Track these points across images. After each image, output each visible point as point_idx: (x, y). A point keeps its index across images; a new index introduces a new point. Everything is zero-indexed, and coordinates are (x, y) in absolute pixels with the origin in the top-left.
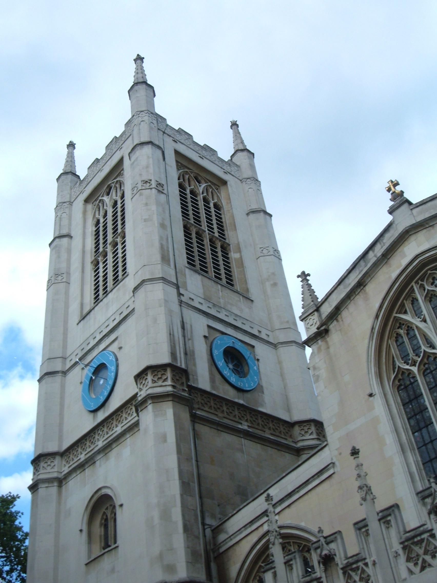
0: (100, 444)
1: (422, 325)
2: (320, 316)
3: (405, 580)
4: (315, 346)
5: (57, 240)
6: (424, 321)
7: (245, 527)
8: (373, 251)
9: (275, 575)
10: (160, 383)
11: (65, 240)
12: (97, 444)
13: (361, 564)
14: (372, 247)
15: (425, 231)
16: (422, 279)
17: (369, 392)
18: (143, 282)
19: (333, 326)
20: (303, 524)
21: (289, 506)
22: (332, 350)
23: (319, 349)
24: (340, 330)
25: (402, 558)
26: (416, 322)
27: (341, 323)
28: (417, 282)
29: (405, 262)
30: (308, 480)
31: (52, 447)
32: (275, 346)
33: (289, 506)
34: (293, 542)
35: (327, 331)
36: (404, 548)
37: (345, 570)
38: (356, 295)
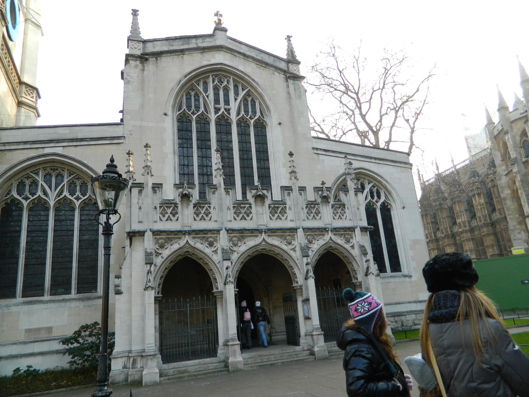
3: (230, 221)
6: (207, 97)
7: (25, 143)
8: (196, 40)
9: (140, 192)
13: (207, 206)
14: (196, 37)
15: (230, 55)
16: (216, 76)
17: (163, 112)
19: (152, 60)
20: (85, 162)
21: (75, 146)
22: (146, 72)
23: (136, 66)
24: (157, 66)
25: (233, 211)
27: (159, 62)
28: (212, 76)
29: (213, 61)
30: (102, 138)
33: (75, 146)
34: (67, 169)
35: (147, 59)
36: (234, 207)
38: (176, 55)
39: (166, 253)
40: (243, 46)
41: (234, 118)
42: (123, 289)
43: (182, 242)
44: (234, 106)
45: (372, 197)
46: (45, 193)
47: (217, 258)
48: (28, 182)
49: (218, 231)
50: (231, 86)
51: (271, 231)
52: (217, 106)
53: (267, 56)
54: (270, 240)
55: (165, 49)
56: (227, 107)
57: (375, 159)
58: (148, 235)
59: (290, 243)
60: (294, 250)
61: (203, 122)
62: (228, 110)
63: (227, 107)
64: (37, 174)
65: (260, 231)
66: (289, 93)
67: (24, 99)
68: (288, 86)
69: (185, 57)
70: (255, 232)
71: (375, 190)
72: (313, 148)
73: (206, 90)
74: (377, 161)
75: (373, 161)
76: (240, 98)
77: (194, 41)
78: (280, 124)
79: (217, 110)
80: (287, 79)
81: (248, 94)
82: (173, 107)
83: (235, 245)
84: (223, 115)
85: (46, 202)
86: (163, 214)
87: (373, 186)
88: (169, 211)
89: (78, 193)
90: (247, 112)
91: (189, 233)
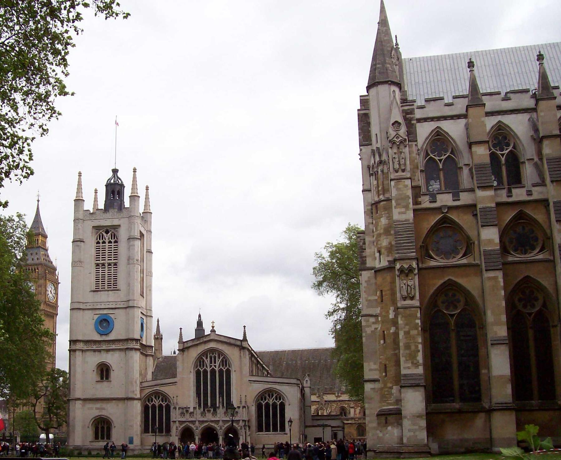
0: (104, 347)
1: (206, 362)
2: (184, 345)
5: (79, 242)
7: (149, 386)
10: (136, 344)
12: (102, 346)
18: (134, 307)
19: (186, 350)
20: (166, 392)
22: (184, 356)
23: (181, 353)
31: (80, 338)
32: (146, 316)
35: (184, 351)
37: (190, 414)
39: (182, 427)
40: (222, 337)
41: (217, 369)
42: (172, 435)
43: (186, 424)
44: (217, 365)
45: (277, 400)
47: (195, 429)
48: (150, 399)
49: (195, 421)
50: (217, 356)
51: (212, 421)
52: (211, 365)
53: (232, 339)
54: (211, 424)
55: (191, 344)
56: (215, 364)
57: (279, 383)
58: (177, 422)
59: (218, 425)
60: (219, 427)
61: (205, 372)
62: (215, 366)
63: (215, 364)
65: (208, 421)
67: (148, 353)
68: (240, 353)
69: (198, 347)
70: (206, 421)
71: (278, 397)
72: (249, 381)
73: (207, 358)
74: (279, 384)
75: (277, 384)
77: (202, 339)
78: (235, 371)
79: (211, 366)
80: (240, 350)
81: (224, 358)
82: (194, 368)
83: (201, 425)
84: (213, 368)
87: (278, 395)
88: (183, 415)
90: (223, 366)
91: (188, 421)
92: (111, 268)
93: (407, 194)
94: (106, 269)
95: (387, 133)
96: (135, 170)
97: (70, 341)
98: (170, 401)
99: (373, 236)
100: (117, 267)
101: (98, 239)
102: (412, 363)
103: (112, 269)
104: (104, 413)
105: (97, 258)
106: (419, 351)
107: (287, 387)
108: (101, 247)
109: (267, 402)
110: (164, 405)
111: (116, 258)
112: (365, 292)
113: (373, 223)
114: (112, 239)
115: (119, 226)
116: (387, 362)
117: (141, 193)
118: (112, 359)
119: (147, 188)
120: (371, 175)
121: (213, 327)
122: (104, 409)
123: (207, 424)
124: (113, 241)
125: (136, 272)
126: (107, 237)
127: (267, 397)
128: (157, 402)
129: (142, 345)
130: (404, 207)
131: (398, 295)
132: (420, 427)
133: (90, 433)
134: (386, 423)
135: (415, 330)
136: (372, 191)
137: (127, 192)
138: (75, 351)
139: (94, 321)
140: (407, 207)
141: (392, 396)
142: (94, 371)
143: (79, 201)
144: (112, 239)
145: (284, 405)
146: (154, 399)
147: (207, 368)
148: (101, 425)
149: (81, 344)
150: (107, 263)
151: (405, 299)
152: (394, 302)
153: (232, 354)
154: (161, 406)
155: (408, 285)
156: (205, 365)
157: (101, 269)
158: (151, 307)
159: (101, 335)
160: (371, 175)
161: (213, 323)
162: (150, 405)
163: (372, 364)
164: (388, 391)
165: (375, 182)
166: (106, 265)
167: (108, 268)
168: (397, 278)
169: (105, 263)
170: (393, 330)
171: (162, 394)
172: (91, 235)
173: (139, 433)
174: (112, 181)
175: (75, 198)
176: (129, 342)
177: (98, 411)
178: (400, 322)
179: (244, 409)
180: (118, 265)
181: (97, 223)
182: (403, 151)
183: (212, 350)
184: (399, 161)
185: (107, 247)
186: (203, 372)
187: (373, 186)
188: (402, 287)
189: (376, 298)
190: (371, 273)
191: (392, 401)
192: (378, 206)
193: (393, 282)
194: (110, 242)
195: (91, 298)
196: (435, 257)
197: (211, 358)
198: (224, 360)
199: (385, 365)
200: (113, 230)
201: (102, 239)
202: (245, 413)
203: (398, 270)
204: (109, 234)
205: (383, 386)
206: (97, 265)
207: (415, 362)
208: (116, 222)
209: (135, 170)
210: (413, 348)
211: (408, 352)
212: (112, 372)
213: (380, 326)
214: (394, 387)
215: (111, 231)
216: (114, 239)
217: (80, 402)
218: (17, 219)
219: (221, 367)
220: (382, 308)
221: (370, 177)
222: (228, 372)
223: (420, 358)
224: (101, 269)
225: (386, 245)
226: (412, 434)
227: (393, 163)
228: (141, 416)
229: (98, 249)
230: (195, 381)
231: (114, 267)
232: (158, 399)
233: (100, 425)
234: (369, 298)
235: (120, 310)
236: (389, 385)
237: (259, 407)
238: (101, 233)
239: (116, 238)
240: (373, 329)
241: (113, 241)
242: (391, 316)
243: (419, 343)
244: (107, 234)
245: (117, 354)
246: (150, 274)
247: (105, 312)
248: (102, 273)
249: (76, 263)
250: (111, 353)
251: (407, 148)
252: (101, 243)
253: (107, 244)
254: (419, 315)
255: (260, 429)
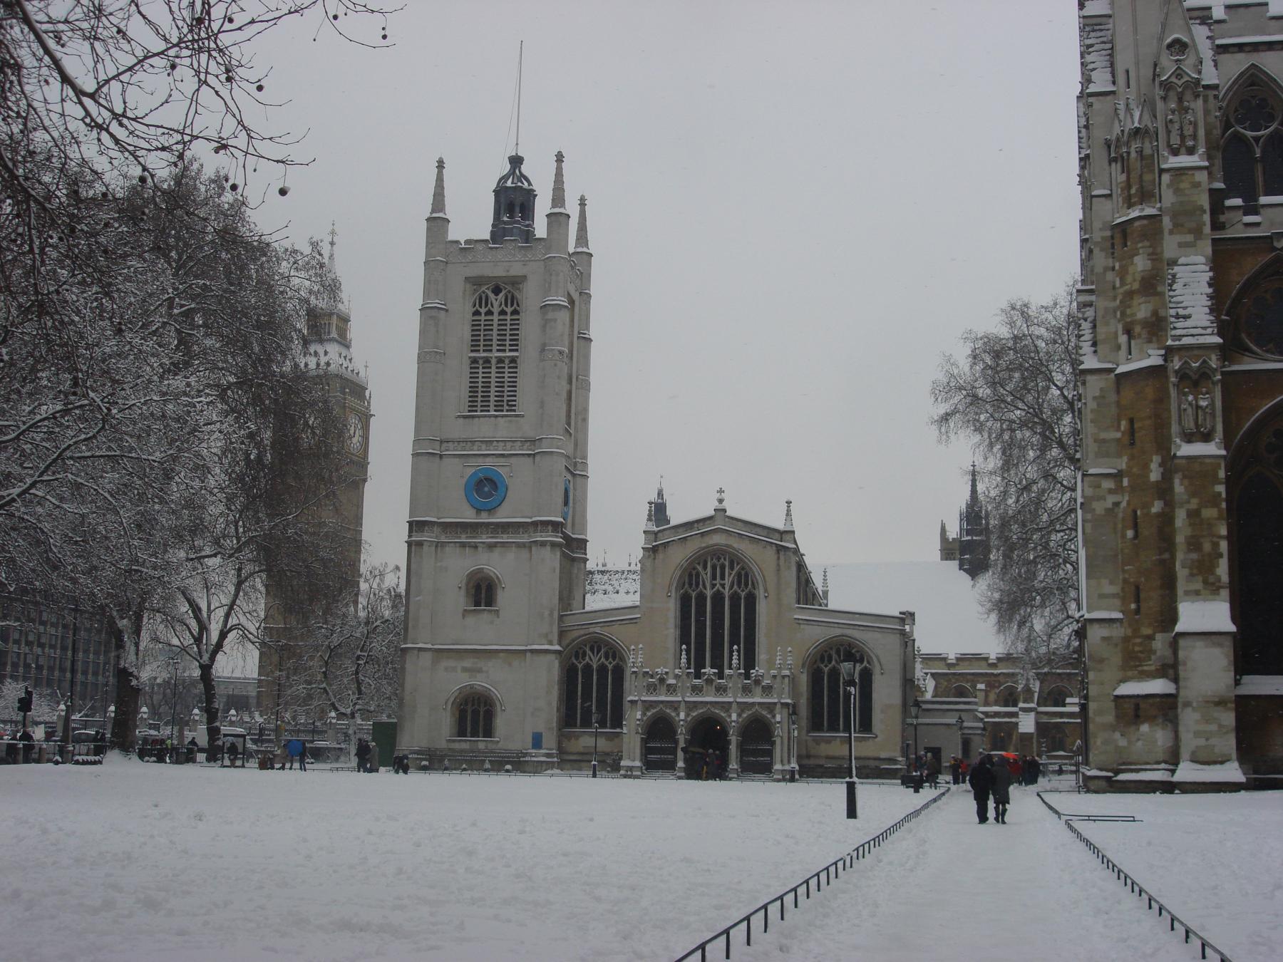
1: (705, 576)
4: (647, 554)
5: (436, 310)
11: (443, 312)
14: (698, 521)
23: (649, 556)
26: (702, 573)
29: (711, 542)
41: (727, 592)
44: (727, 582)
46: (591, 660)
48: (581, 652)
50: (727, 563)
52: (714, 582)
56: (722, 582)
61: (701, 598)
63: (722, 582)
64: (586, 646)
66: (778, 565)
68: (779, 558)
73: (705, 568)
76: (734, 572)
79: (713, 586)
80: (778, 551)
81: (743, 568)
84: (718, 590)
85: (591, 666)
86: (648, 690)
89: (610, 659)
92: (504, 367)
93: (1199, 203)
94: (494, 370)
95: (1155, 65)
96: (560, 158)
97: (410, 523)
98: (622, 659)
99: (1115, 298)
100: (516, 367)
101: (477, 306)
102: (1205, 582)
103: (506, 370)
104: (480, 682)
105: (474, 347)
106: (1221, 555)
107: (877, 635)
108: (482, 323)
109: (834, 667)
110: (610, 667)
111: (515, 346)
112: (1092, 422)
113: (1113, 269)
114: (506, 306)
115: (525, 277)
116: (1143, 579)
117: (572, 208)
118: (499, 564)
119: (582, 203)
120: (1112, 161)
121: (721, 501)
122: (480, 671)
123: (705, 710)
124: (509, 310)
125: (559, 377)
126: (496, 302)
127: (834, 656)
128: (595, 659)
129: (566, 537)
130: (1190, 232)
131: (1175, 428)
132: (1220, 726)
133: (447, 722)
134: (1137, 716)
135: (1212, 507)
136: (1114, 196)
137: (542, 207)
138: (420, 544)
139: (465, 480)
140: (1198, 232)
141: (1153, 657)
142: (460, 588)
143: (437, 223)
144: (506, 306)
145: (871, 675)
146: (589, 652)
147: (705, 589)
148: (473, 705)
149: (435, 529)
150: (496, 357)
151: (1189, 438)
152: (1163, 445)
153: (761, 560)
154: (602, 669)
155: (1198, 407)
156: (701, 583)
157: (481, 370)
158: (585, 457)
159: (479, 511)
160: (1115, 160)
161: (721, 491)
162: (580, 666)
163: (1105, 582)
164: (1140, 644)
165: (1123, 178)
166: (494, 361)
167: (497, 368)
168: (1173, 393)
169: (491, 357)
170: (1157, 507)
171: (607, 644)
172: (461, 294)
173: (555, 724)
174: (509, 183)
175: (428, 215)
176: (539, 528)
177: (466, 675)
178: (1179, 488)
179: (786, 680)
180: (518, 362)
181: (474, 271)
182: (1192, 105)
183: (718, 553)
184: (1181, 128)
185: (496, 323)
186: (696, 599)
187: (1117, 186)
188: (1185, 410)
189: (1119, 435)
190: (1107, 379)
191: (1153, 668)
192: (1128, 231)
193: (1161, 399)
194: (503, 313)
195: (458, 429)
196: (1255, 348)
197: (714, 568)
198: (743, 573)
199: (1137, 588)
200: (509, 288)
201: (486, 305)
202: (787, 689)
203: (1176, 372)
204: (501, 295)
205: (1129, 632)
206: (474, 361)
207: (1211, 579)
208: (516, 270)
209: (560, 158)
210: (1207, 547)
211: (1194, 556)
212: (499, 592)
213: (1127, 498)
214: (1159, 636)
215: (506, 289)
216: (512, 305)
217: (428, 656)
218: (307, 250)
219: (735, 587)
220: (1132, 458)
221: (1110, 164)
222: (751, 600)
223: (1223, 569)
224: (481, 370)
225: (1145, 318)
226: (1202, 742)
227: (1169, 132)
228: (560, 689)
229: (475, 326)
230: (678, 614)
231: (511, 365)
232: (597, 654)
233: (470, 705)
234: (1103, 435)
235: (522, 459)
236: (1147, 631)
237: (816, 678)
238: (484, 292)
239: (515, 305)
240: (1110, 506)
241: (509, 310)
242: (1155, 475)
243: (1221, 537)
244: (497, 294)
245: (511, 555)
246: (586, 386)
247: (489, 462)
248: (483, 377)
249: (429, 357)
250: (498, 550)
251: (1200, 102)
252: (483, 315)
253: (496, 317)
254: (1222, 474)
255: (816, 725)
